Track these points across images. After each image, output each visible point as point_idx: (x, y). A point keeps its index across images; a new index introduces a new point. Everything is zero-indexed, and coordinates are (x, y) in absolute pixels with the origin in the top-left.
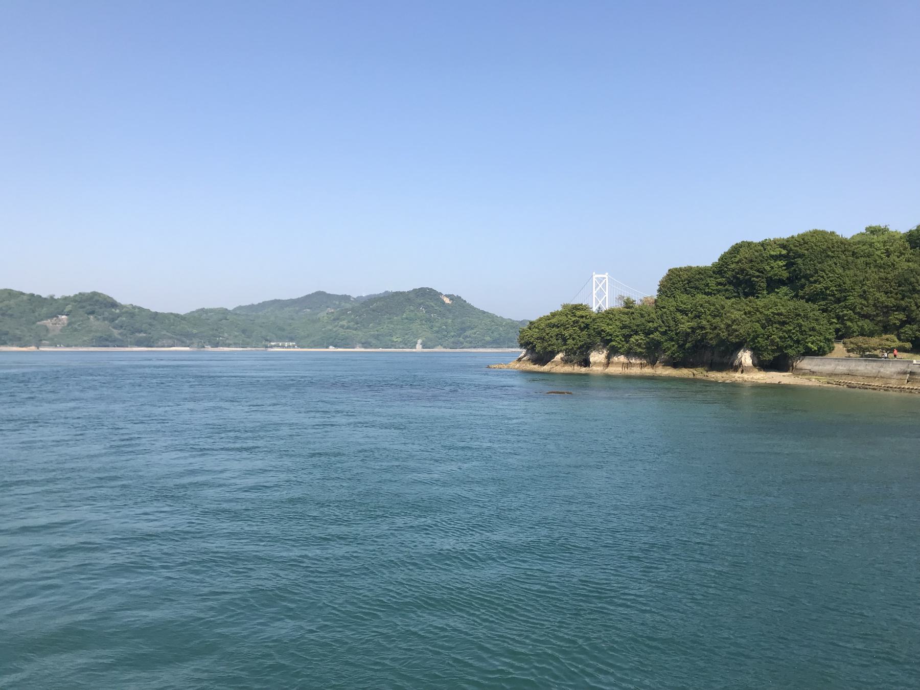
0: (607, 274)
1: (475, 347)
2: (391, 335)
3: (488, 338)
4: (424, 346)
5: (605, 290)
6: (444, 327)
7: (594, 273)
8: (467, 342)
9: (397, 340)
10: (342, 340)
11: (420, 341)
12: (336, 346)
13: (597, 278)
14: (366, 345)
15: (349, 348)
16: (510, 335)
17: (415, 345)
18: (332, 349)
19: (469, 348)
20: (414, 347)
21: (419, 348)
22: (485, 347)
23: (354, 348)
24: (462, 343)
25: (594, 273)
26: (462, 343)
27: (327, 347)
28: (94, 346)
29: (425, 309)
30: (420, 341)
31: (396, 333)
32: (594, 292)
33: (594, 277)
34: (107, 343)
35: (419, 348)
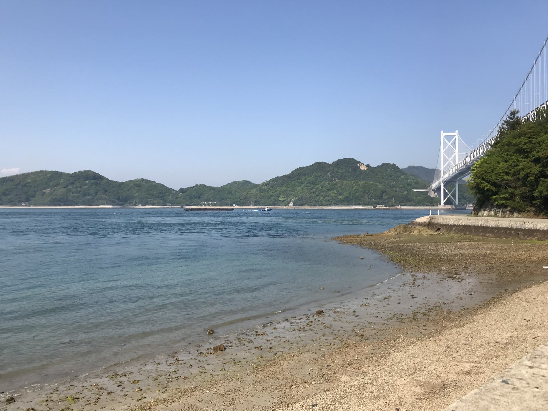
0: (457, 131)
1: (330, 205)
2: (279, 197)
3: (340, 197)
4: (294, 205)
6: (320, 188)
7: (442, 132)
8: (325, 201)
9: (281, 199)
10: (242, 200)
11: (294, 199)
12: (238, 205)
13: (445, 137)
14: (257, 203)
15: (245, 206)
17: (289, 203)
19: (327, 205)
20: (287, 205)
21: (291, 206)
22: (338, 205)
23: (248, 206)
24: (321, 201)
25: (442, 132)
26: (321, 201)
27: (232, 205)
28: (49, 205)
29: (330, 174)
30: (294, 199)
31: (284, 194)
32: (442, 151)
34: (59, 203)
35: (291, 206)
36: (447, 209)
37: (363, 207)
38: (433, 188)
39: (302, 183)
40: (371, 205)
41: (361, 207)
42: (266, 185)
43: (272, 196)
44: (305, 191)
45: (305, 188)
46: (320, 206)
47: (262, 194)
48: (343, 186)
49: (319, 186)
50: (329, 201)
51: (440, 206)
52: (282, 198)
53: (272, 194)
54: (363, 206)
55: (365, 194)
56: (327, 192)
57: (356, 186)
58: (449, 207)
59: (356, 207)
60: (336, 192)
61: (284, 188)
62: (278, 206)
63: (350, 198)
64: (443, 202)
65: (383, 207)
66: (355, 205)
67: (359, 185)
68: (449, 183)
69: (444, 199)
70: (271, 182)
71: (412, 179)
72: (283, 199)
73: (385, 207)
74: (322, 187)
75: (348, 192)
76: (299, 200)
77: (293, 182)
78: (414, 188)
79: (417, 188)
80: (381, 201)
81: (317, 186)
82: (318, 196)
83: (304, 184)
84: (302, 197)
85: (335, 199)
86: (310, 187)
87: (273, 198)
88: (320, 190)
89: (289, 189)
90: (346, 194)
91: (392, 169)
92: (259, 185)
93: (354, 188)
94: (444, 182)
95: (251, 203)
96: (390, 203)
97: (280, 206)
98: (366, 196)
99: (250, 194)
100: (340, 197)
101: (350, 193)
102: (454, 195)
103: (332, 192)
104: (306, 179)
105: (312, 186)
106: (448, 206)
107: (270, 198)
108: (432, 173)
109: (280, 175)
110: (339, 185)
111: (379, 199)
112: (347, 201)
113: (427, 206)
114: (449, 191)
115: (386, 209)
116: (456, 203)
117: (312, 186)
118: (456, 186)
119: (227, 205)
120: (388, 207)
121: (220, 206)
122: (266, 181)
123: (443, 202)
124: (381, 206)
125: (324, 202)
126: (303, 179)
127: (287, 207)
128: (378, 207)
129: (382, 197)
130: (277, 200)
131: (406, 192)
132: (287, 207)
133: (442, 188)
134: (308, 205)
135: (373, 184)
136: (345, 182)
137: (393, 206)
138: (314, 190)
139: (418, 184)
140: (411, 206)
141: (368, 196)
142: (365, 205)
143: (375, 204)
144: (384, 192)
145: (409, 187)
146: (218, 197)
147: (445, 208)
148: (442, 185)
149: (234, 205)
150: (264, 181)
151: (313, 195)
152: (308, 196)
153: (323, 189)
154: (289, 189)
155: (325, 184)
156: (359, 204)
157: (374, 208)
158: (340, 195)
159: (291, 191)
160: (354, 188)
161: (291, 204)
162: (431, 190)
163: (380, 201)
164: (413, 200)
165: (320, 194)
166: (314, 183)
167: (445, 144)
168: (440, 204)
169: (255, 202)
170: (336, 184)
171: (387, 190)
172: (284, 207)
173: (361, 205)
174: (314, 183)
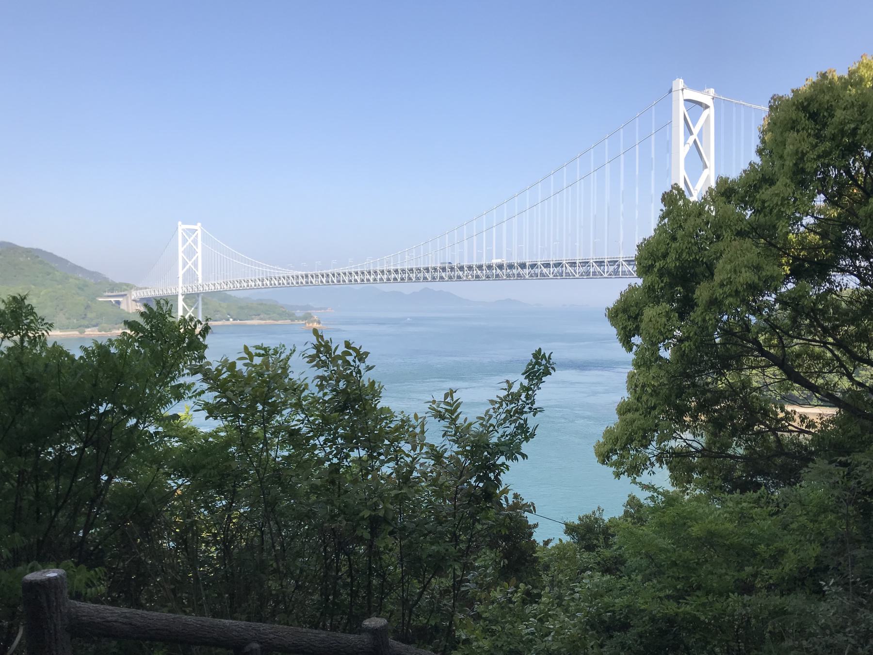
5: (197, 248)
32: (181, 249)
37: (61, 333)
38: (133, 298)
40: (73, 328)
54: (61, 332)
71: (75, 279)
73: (100, 331)
91: (27, 257)
94: (183, 295)
120: (103, 333)
124: (92, 331)
129: (85, 315)
137: (110, 330)
139: (87, 286)
141: (64, 315)
143: (81, 327)
144: (88, 307)
148: (180, 298)
157: (81, 333)
162: (130, 301)
163: (86, 322)
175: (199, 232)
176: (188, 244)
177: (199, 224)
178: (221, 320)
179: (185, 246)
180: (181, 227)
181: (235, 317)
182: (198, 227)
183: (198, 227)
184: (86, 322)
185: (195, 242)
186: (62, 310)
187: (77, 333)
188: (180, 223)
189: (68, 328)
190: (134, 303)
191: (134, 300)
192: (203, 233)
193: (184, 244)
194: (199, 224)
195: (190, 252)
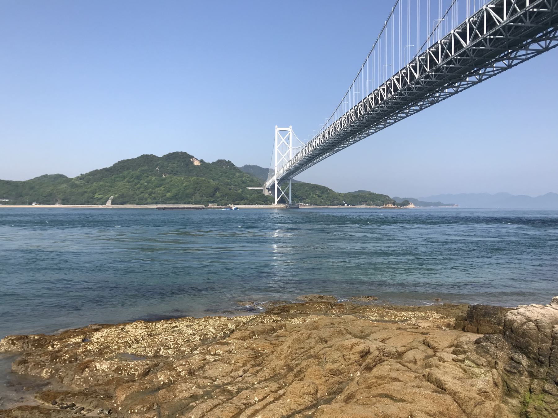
1: (156, 203)
2: (94, 193)
3: (168, 195)
6: (146, 184)
9: (98, 196)
10: (45, 197)
11: (112, 197)
16: (188, 191)
17: (106, 202)
18: (35, 205)
19: (152, 204)
20: (104, 203)
21: (109, 205)
22: (165, 203)
23: (54, 204)
24: (146, 199)
26: (146, 199)
27: (31, 204)
30: (112, 197)
33: (277, 133)
36: (280, 208)
39: (124, 178)
40: (203, 204)
41: (191, 206)
42: (81, 179)
43: (85, 192)
44: (128, 187)
45: (127, 183)
46: (145, 204)
47: (74, 190)
48: (173, 182)
49: (144, 182)
50: (155, 198)
51: (274, 204)
52: (99, 195)
53: (86, 190)
55: (196, 191)
56: (153, 189)
57: (187, 182)
58: (282, 205)
59: (186, 206)
60: (163, 189)
61: (101, 183)
62: (92, 205)
63: (180, 196)
64: (276, 200)
65: (215, 205)
66: (185, 203)
67: (190, 181)
68: (283, 181)
69: (278, 198)
70: (87, 176)
72: (99, 197)
74: (148, 183)
75: (177, 189)
76: (119, 197)
77: (113, 177)
78: (249, 186)
79: (252, 186)
80: (214, 199)
81: (142, 182)
82: (143, 193)
83: (126, 180)
84: (123, 195)
85: (162, 197)
86: (134, 183)
87: (86, 195)
88: (145, 186)
89: (108, 184)
90: (174, 191)
92: (72, 179)
93: (184, 185)
95: (57, 201)
96: (223, 201)
97: (95, 205)
98: (198, 194)
99: (57, 189)
100: (168, 195)
101: (179, 190)
102: (287, 194)
103: (158, 188)
104: (129, 173)
105: (136, 181)
106: (282, 204)
107: (83, 195)
108: (266, 173)
109: (99, 168)
110: (168, 181)
111: (212, 197)
112: (176, 199)
113: (261, 204)
114: (283, 190)
115: (218, 208)
116: (289, 202)
117: (136, 181)
118: (289, 184)
119: (23, 203)
120: (220, 206)
121: (14, 204)
122: (81, 174)
123: (276, 200)
124: (213, 205)
125: (149, 200)
126: (125, 173)
127: (104, 206)
128: (210, 205)
129: (214, 194)
130: (92, 198)
131: (241, 190)
132: (104, 206)
133: (276, 186)
134: (130, 204)
135: (205, 180)
136: (175, 177)
138: (138, 186)
140: (244, 204)
141: (199, 194)
142: (195, 203)
144: (217, 189)
145: (243, 185)
146: (14, 193)
147: (279, 206)
148: (276, 183)
149: (34, 204)
150: (78, 175)
151: (137, 192)
152: (131, 193)
153: (150, 184)
154: (108, 184)
155: (151, 180)
156: (189, 203)
157: (206, 206)
158: (167, 192)
159: (111, 187)
160: (184, 185)
161: (109, 202)
163: (213, 199)
164: (247, 199)
165: (145, 191)
166: (139, 178)
167: (280, 140)
168: (274, 203)
169: (63, 200)
170: (164, 180)
171: (219, 187)
172: (100, 206)
173: (192, 203)
174: (139, 178)
175: (290, 133)
176: (282, 142)
177: (291, 127)
178: (338, 204)
179: (279, 145)
180: (277, 129)
181: (348, 203)
182: (290, 129)
183: (290, 129)
184: (213, 199)
185: (288, 140)
186: (198, 191)
187: (203, 206)
188: (276, 126)
189: (200, 203)
190: (267, 190)
191: (267, 188)
192: (293, 134)
193: (279, 143)
194: (291, 127)
195: (284, 148)
